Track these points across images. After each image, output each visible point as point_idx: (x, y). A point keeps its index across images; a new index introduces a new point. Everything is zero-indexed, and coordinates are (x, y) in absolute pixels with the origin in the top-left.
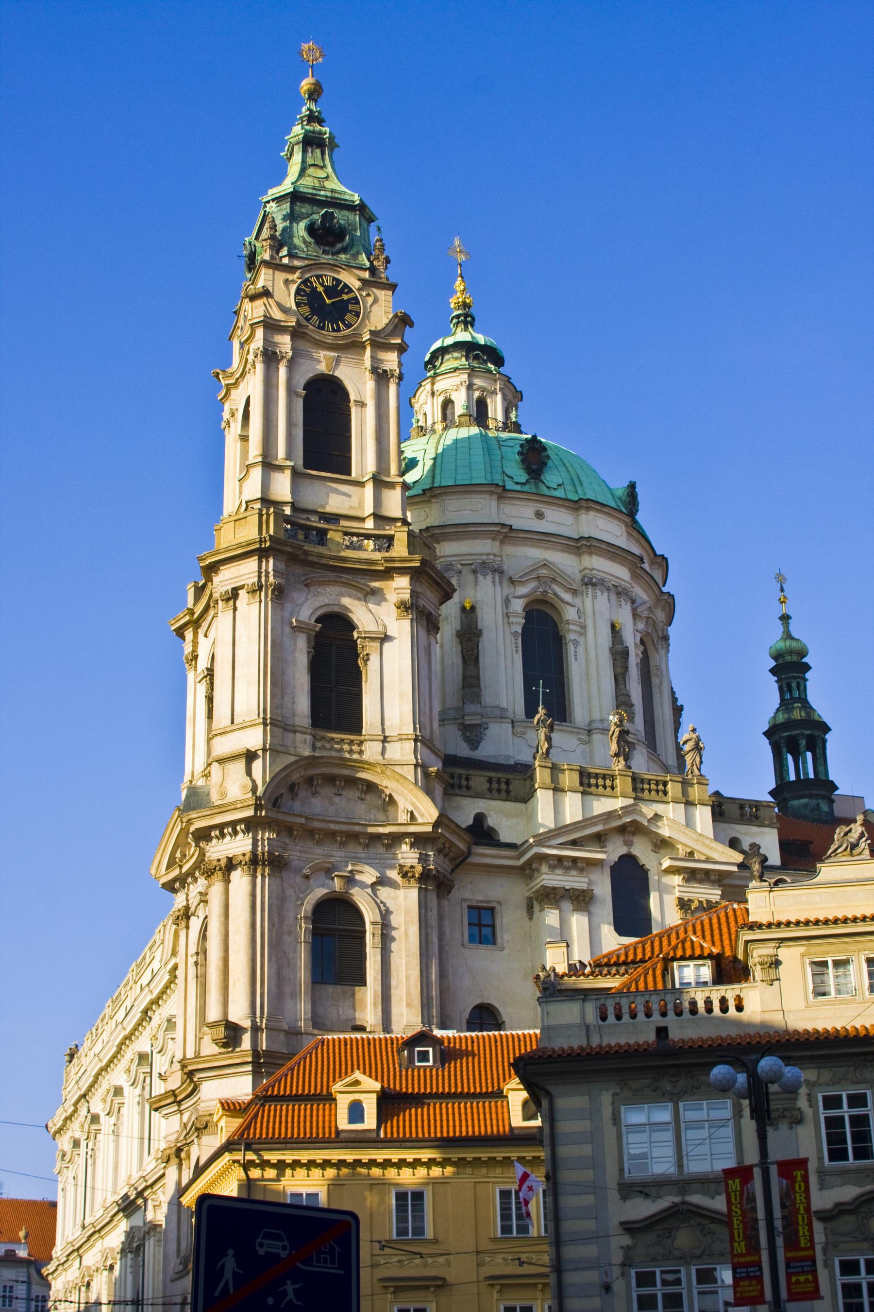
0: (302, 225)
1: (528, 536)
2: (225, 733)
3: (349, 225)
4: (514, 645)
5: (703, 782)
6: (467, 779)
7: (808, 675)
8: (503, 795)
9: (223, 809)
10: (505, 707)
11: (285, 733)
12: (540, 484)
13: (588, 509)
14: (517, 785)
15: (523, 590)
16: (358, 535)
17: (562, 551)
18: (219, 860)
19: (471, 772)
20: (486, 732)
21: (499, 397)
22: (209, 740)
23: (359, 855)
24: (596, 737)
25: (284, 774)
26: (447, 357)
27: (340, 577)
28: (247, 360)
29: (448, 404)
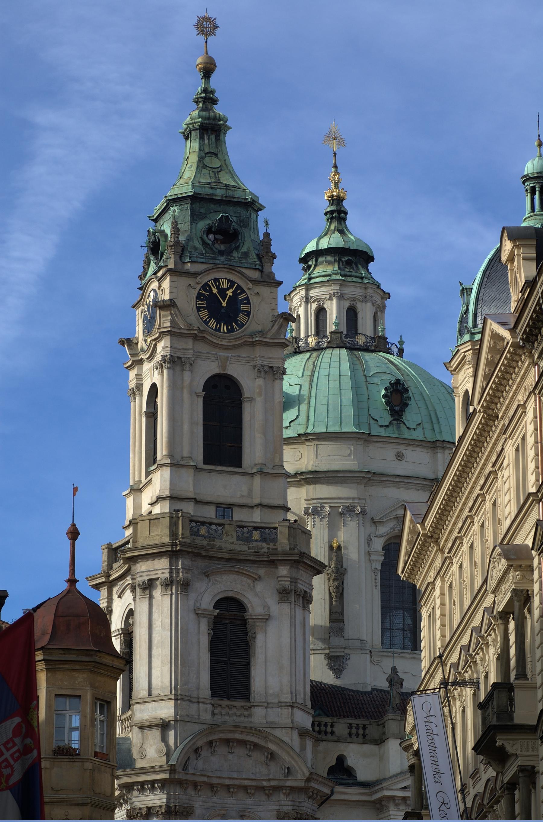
0: (202, 225)
1: (389, 479)
2: (144, 702)
3: (241, 221)
4: (374, 580)
6: (332, 726)
8: (361, 738)
9: (144, 771)
10: (364, 638)
11: (191, 704)
12: (402, 425)
13: (443, 448)
15: (383, 530)
16: (247, 527)
17: (418, 490)
18: (140, 809)
19: (335, 720)
20: (348, 662)
21: (369, 305)
23: (247, 802)
25: (192, 743)
26: (320, 259)
27: (234, 568)
29: (321, 312)
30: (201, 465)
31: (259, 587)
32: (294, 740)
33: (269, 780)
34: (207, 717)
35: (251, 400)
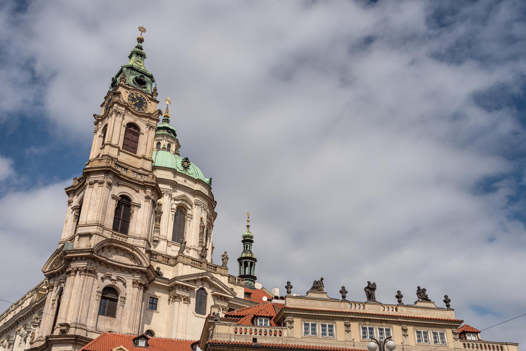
0: (133, 77)
5: (227, 269)
7: (252, 244)
14: (172, 261)
22: (76, 228)
24: (192, 251)
28: (108, 112)
29: (159, 144)
30: (121, 149)
31: (138, 194)
32: (144, 251)
33: (132, 265)
34: (109, 237)
35: (143, 134)
